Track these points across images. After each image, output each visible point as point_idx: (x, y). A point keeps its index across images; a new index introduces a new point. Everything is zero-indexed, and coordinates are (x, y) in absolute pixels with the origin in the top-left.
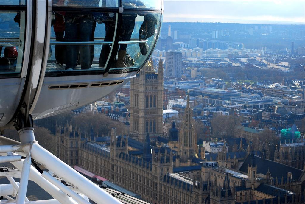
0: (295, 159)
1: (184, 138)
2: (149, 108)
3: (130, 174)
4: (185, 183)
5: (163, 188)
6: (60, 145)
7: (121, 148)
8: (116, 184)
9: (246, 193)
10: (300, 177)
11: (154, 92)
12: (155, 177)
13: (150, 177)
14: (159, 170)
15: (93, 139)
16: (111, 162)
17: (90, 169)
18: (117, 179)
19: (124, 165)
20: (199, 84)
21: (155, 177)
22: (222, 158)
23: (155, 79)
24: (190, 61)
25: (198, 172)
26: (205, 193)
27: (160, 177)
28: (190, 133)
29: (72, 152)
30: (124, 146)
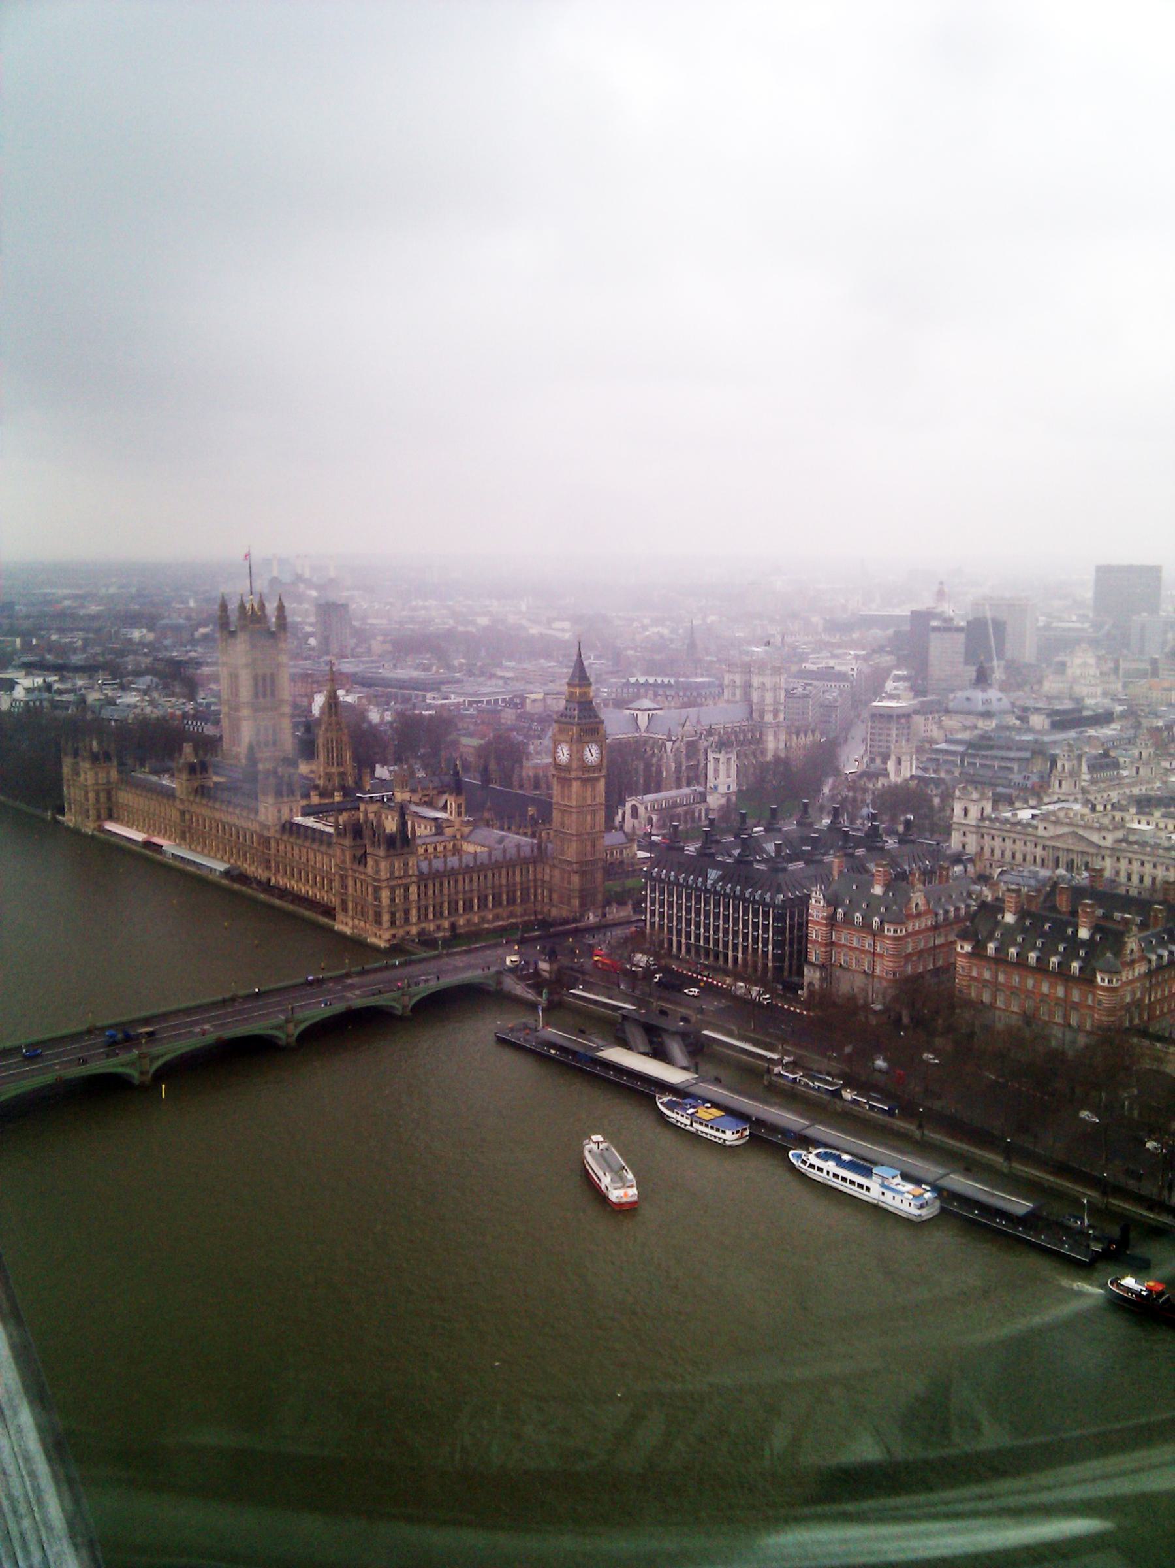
2: (261, 700)
3: (218, 826)
4: (322, 833)
5: (282, 847)
7: (199, 776)
9: (445, 847)
12: (267, 827)
15: (142, 765)
17: (137, 827)
20: (383, 666)
24: (373, 625)
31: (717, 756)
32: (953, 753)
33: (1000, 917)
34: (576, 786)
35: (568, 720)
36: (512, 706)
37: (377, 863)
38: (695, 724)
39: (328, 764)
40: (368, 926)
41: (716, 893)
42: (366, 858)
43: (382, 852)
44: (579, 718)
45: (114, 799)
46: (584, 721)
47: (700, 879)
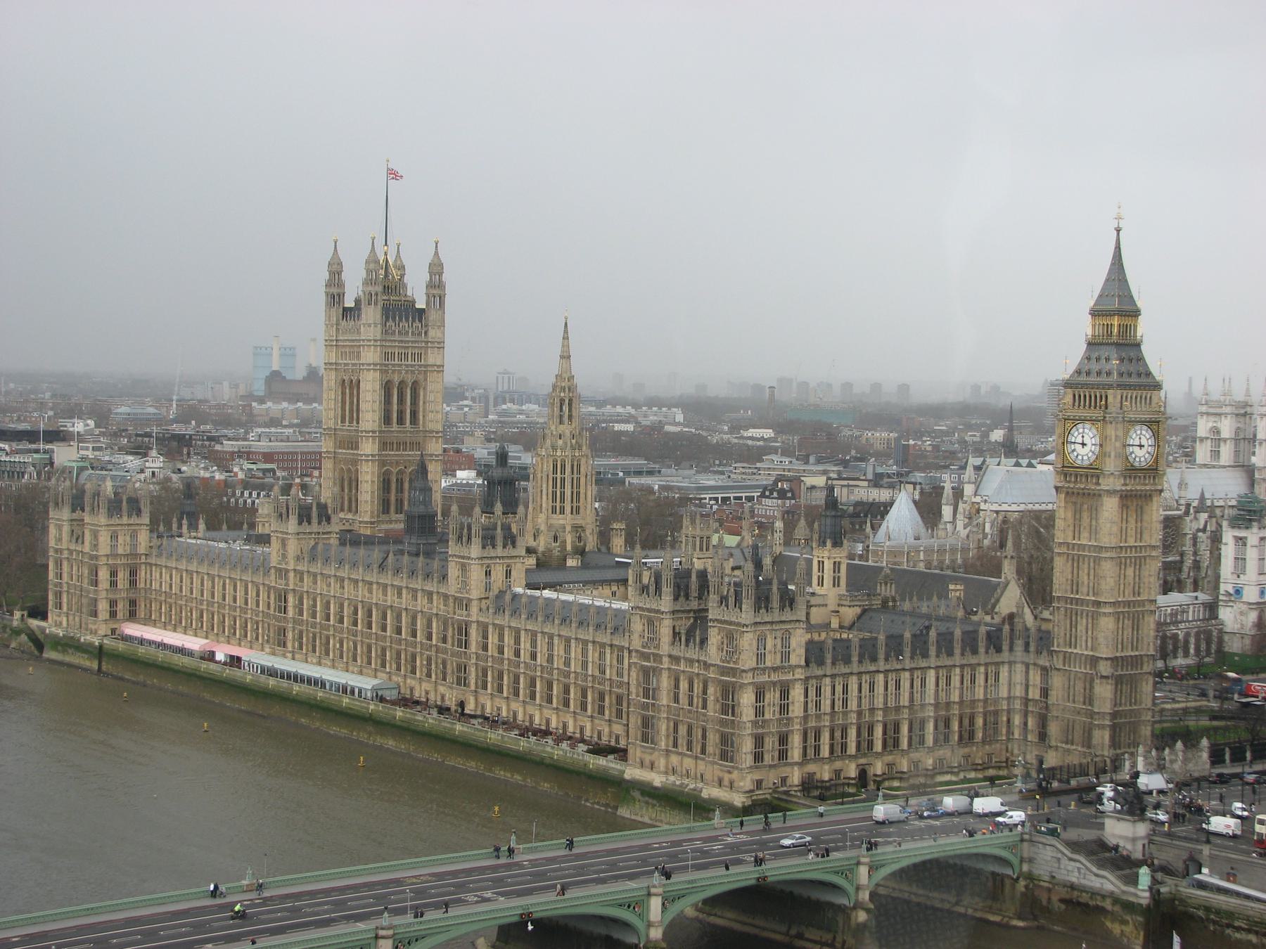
1: (551, 483)
2: (395, 427)
3: (356, 613)
5: (493, 639)
6: (66, 552)
7: (315, 527)
8: (293, 659)
10: (993, 601)
11: (413, 372)
12: (463, 603)
13: (438, 606)
14: (476, 574)
15: (193, 526)
16: (273, 584)
18: (296, 644)
19: (329, 585)
21: (461, 600)
22: (698, 543)
23: (417, 324)
25: (614, 588)
26: (683, 612)
27: (481, 599)
28: (572, 466)
29: (114, 574)
30: (324, 523)
31: (1242, 534)
34: (1110, 506)
35: (1093, 379)
36: (775, 494)
37: (730, 637)
39: (554, 511)
42: (705, 630)
43: (746, 615)
44: (1121, 375)
46: (1126, 379)
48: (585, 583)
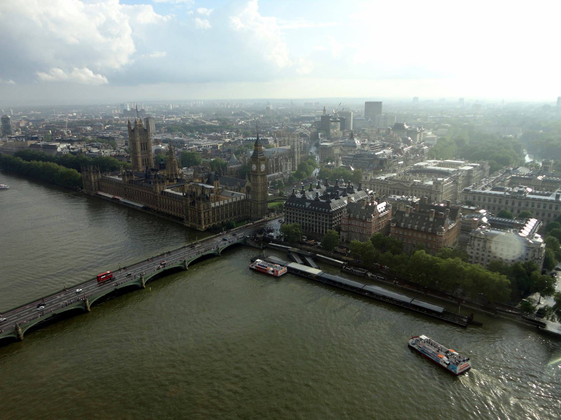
0: (237, 174)
2: (143, 151)
4: (176, 195)
5: (162, 199)
8: (129, 200)
9: (214, 197)
12: (156, 193)
13: (151, 193)
15: (108, 173)
17: (109, 193)
29: (95, 183)
32: (351, 159)
33: (404, 215)
35: (255, 157)
38: (276, 152)
40: (196, 225)
41: (309, 210)
42: (195, 204)
43: (201, 201)
45: (100, 184)
47: (304, 206)
48: (177, 187)
